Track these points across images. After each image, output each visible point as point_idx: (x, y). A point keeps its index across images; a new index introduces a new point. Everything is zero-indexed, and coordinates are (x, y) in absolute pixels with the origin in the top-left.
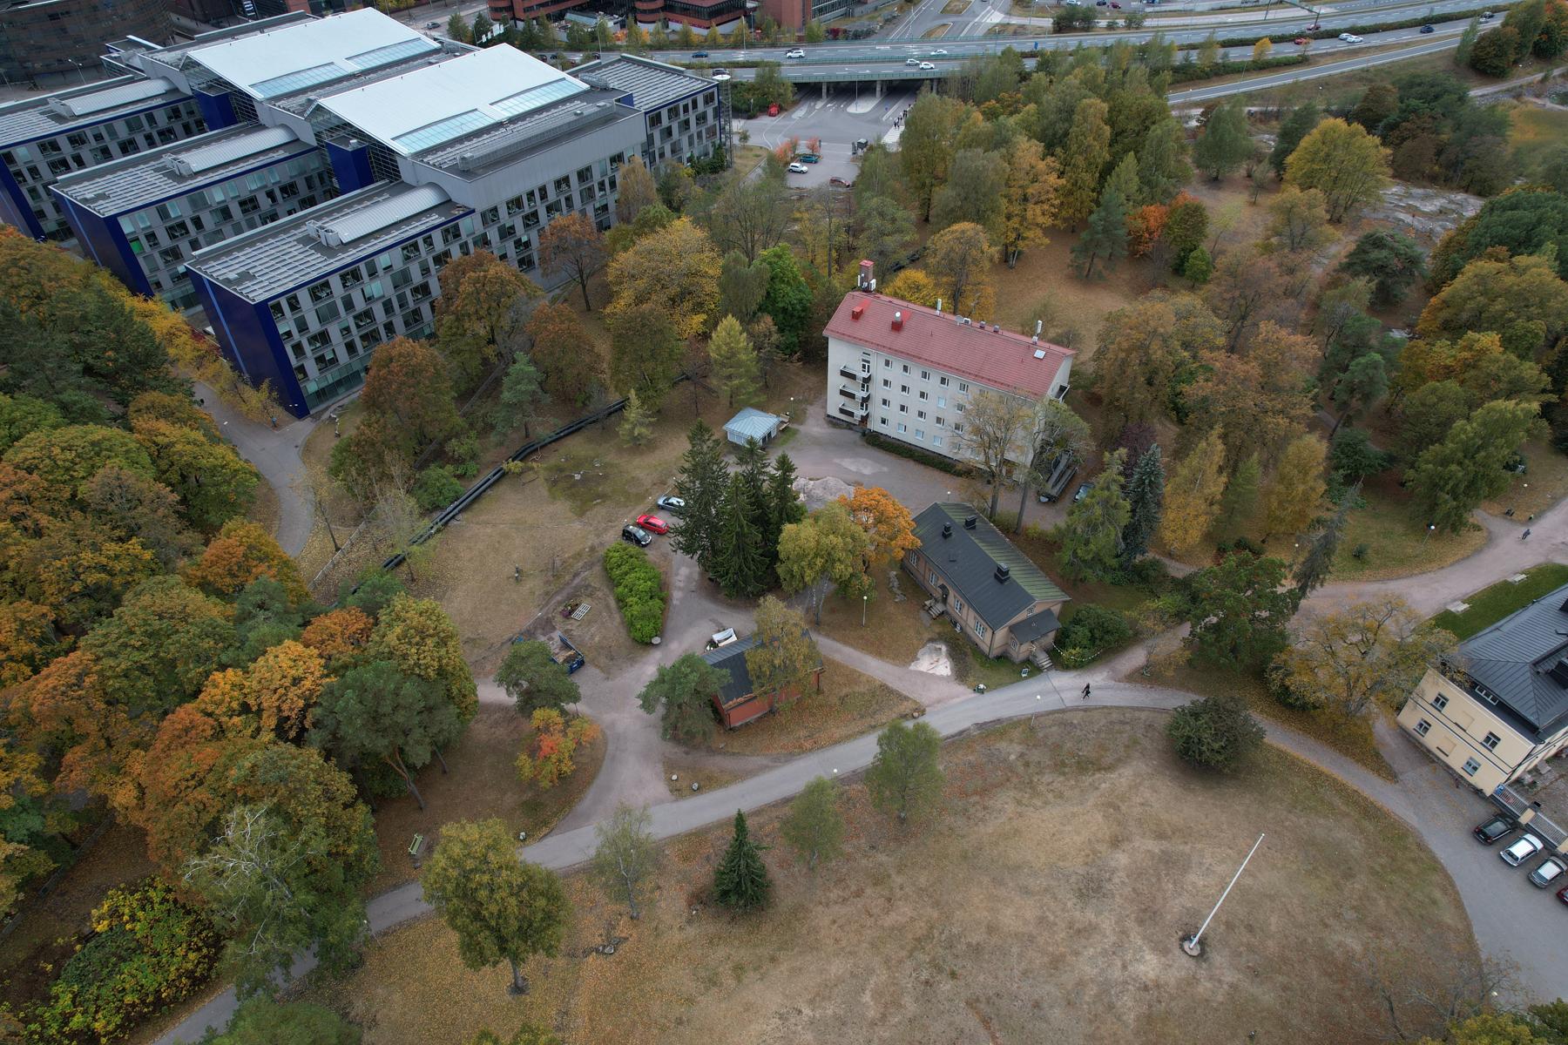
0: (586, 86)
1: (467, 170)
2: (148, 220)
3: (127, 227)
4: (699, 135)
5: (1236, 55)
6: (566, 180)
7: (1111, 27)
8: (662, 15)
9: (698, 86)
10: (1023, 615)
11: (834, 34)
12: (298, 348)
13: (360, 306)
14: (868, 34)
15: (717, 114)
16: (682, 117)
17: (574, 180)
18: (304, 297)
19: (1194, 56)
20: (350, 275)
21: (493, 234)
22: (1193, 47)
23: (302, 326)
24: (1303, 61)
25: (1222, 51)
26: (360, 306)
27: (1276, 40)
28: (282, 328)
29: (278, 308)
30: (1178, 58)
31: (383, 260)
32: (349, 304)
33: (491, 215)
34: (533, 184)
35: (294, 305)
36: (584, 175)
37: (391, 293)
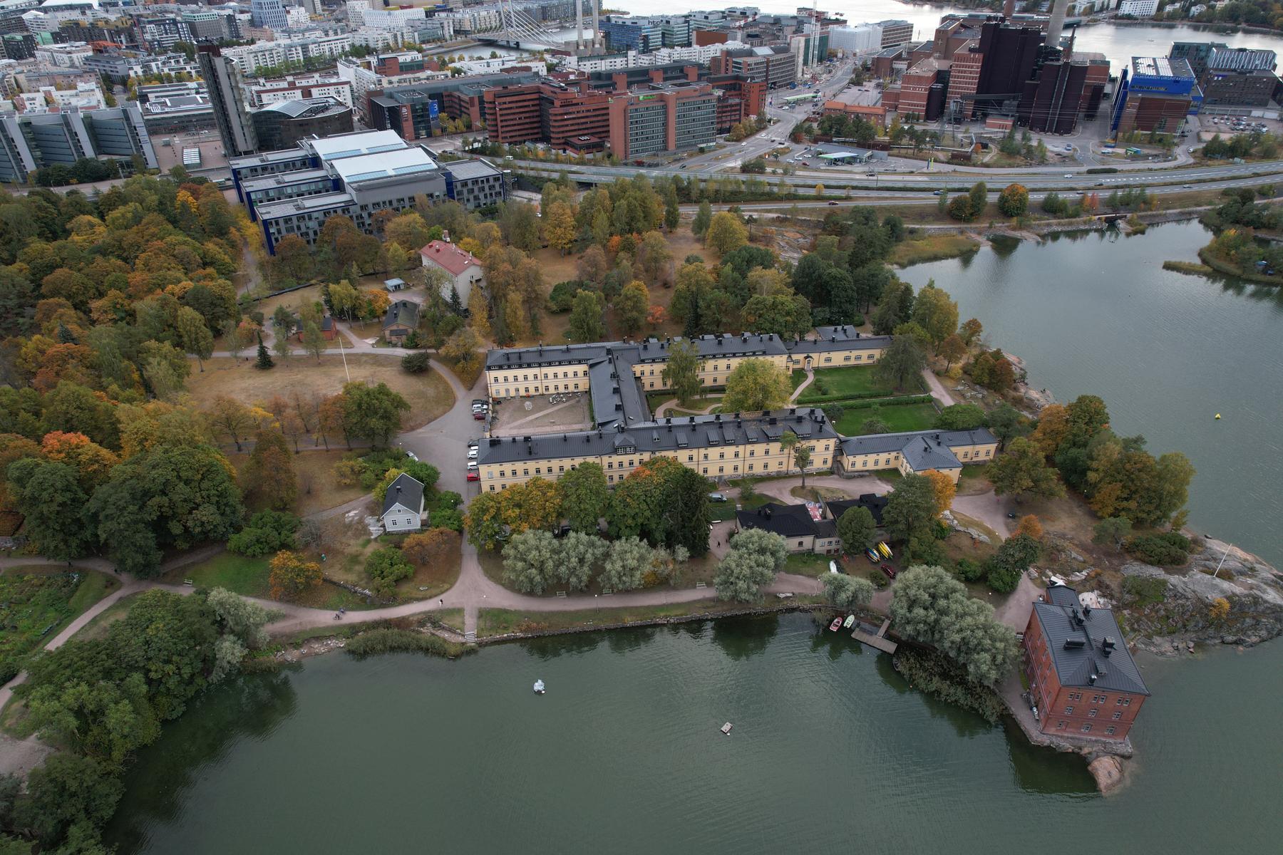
0: (436, 167)
1: (359, 190)
2: (260, 195)
3: (253, 196)
4: (491, 194)
5: (801, 191)
6: (403, 200)
7: (774, 173)
8: (562, 146)
9: (491, 172)
10: (395, 328)
11: (640, 164)
12: (277, 240)
13: (304, 229)
14: (657, 165)
15: (502, 186)
16: (480, 185)
17: (407, 200)
18: (281, 222)
19: (776, 189)
20: (301, 217)
21: (365, 214)
22: (776, 185)
23: (279, 231)
24: (848, 198)
25: (793, 189)
26: (304, 229)
27: (827, 187)
28: (272, 231)
29: (271, 223)
30: (767, 189)
31: (315, 215)
32: (299, 228)
33: (363, 208)
34: (387, 198)
35: (277, 223)
36: (412, 199)
37: (317, 228)
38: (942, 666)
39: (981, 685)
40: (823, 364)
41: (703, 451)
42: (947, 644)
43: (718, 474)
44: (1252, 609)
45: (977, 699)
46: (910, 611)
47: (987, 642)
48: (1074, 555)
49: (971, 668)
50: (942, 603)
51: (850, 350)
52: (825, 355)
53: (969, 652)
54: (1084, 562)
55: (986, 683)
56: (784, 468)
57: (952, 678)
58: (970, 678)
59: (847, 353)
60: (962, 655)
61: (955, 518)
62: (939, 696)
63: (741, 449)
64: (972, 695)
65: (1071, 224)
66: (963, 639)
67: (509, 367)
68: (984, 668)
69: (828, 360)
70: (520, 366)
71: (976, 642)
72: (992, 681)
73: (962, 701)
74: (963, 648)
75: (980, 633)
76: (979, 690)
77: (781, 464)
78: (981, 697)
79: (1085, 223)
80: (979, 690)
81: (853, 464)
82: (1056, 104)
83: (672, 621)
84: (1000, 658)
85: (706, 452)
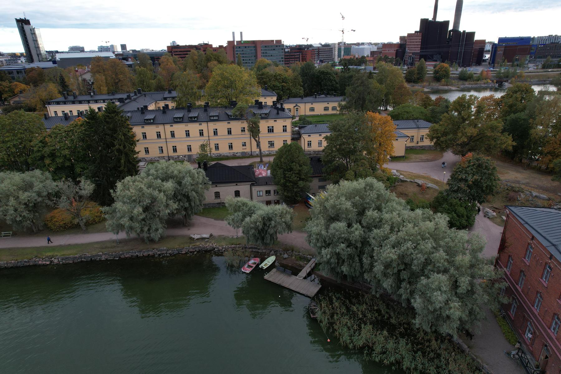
38: (379, 311)
39: (439, 337)
40: (308, 113)
41: (169, 128)
42: (378, 268)
43: (187, 153)
45: (432, 360)
46: (327, 228)
47: (441, 254)
48: (534, 194)
49: (417, 303)
50: (371, 213)
51: (328, 102)
52: (309, 106)
53: (414, 278)
54: (549, 199)
55: (445, 329)
56: (247, 150)
57: (392, 329)
58: (417, 322)
59: (325, 105)
60: (404, 284)
61: (401, 174)
62: (370, 354)
63: (204, 126)
64: (424, 354)
65: (477, 84)
66: (402, 257)
67: (65, 103)
68: (439, 298)
69: (312, 109)
70: (73, 103)
71: (422, 258)
72: (456, 324)
73: (406, 364)
74: (405, 275)
75: (429, 245)
76: (434, 344)
77: (244, 145)
78: (438, 356)
79: (485, 83)
80: (434, 344)
81: (309, 144)
82: (462, 45)
83: (56, 261)
84: (464, 282)
85: (172, 129)
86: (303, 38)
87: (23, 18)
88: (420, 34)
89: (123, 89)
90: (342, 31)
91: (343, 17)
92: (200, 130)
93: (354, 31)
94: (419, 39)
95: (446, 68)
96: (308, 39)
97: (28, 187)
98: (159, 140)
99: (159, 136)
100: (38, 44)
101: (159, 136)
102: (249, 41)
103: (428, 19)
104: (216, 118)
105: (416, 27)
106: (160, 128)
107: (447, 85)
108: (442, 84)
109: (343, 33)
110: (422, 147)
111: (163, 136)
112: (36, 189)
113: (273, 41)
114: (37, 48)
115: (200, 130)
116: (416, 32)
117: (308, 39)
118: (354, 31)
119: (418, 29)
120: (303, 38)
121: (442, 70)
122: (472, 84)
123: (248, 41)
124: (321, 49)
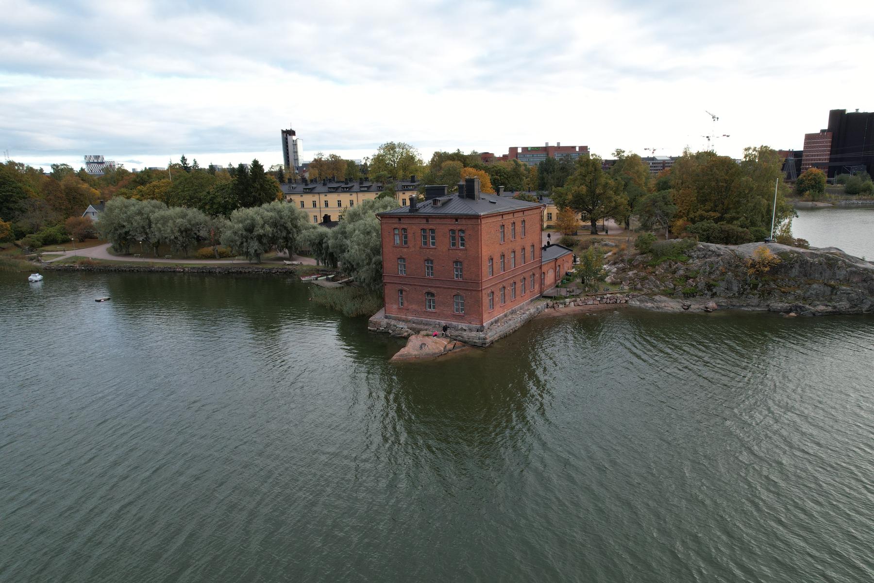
41: (323, 198)
44: (828, 273)
85: (326, 198)
86: (646, 149)
87: (289, 129)
88: (830, 134)
89: (317, 176)
90: (708, 137)
91: (713, 117)
92: (350, 201)
93: (728, 136)
94: (827, 142)
95: (815, 175)
96: (654, 150)
97: (184, 216)
98: (314, 209)
99: (315, 205)
100: (297, 156)
101: (315, 205)
102: (539, 147)
103: (844, 111)
104: (366, 189)
105: (823, 124)
106: (316, 198)
107: (813, 200)
108: (804, 199)
109: (709, 140)
110: (584, 227)
111: (318, 205)
112: (188, 217)
113: (574, 148)
114: (296, 160)
115: (350, 201)
116: (823, 131)
117: (654, 150)
118: (728, 136)
119: (826, 127)
120: (646, 149)
121: (810, 178)
122: (864, 199)
123: (537, 148)
124: (668, 163)
